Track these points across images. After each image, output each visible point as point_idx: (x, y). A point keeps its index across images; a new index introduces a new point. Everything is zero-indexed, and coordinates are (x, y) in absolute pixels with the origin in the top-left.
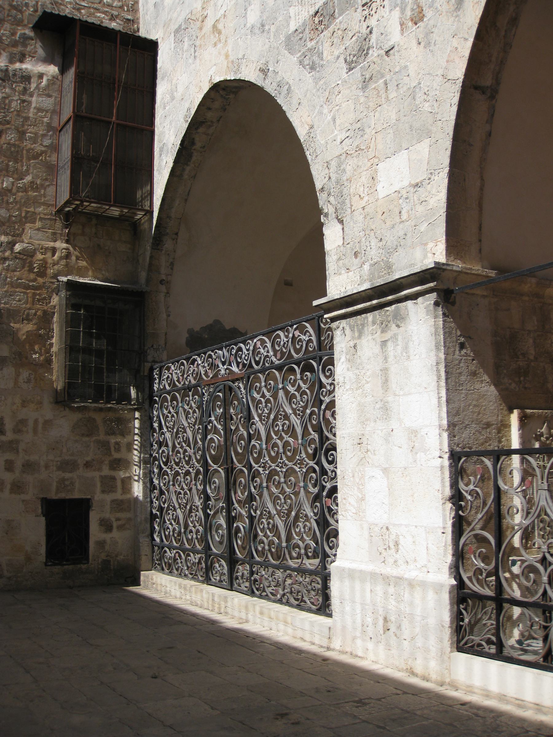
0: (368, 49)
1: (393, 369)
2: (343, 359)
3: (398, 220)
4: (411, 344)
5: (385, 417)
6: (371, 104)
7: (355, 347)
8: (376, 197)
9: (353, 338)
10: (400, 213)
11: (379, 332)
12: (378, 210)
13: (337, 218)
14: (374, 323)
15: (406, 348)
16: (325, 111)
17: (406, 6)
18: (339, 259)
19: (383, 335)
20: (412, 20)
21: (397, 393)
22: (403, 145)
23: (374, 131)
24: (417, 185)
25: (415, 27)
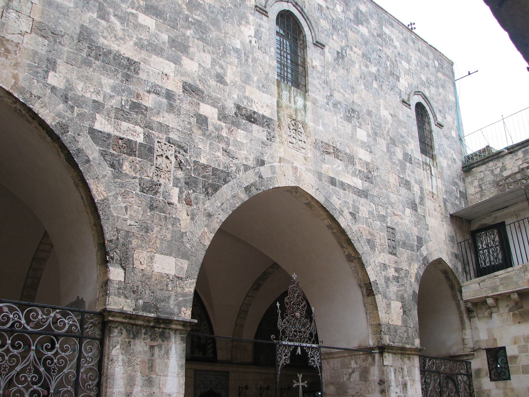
0: (157, 192)
1: (158, 361)
2: (118, 347)
3: (165, 287)
4: (170, 352)
5: (149, 385)
6: (155, 221)
7: (129, 342)
8: (153, 269)
9: (129, 337)
10: (167, 285)
11: (149, 340)
12: (153, 276)
13: (121, 264)
14: (145, 334)
15: (167, 353)
16: (120, 198)
17: (183, 192)
18: (120, 288)
19: (152, 342)
20: (185, 201)
21: (159, 374)
22: (173, 255)
23: (155, 235)
24: (179, 278)
25: (186, 206)
